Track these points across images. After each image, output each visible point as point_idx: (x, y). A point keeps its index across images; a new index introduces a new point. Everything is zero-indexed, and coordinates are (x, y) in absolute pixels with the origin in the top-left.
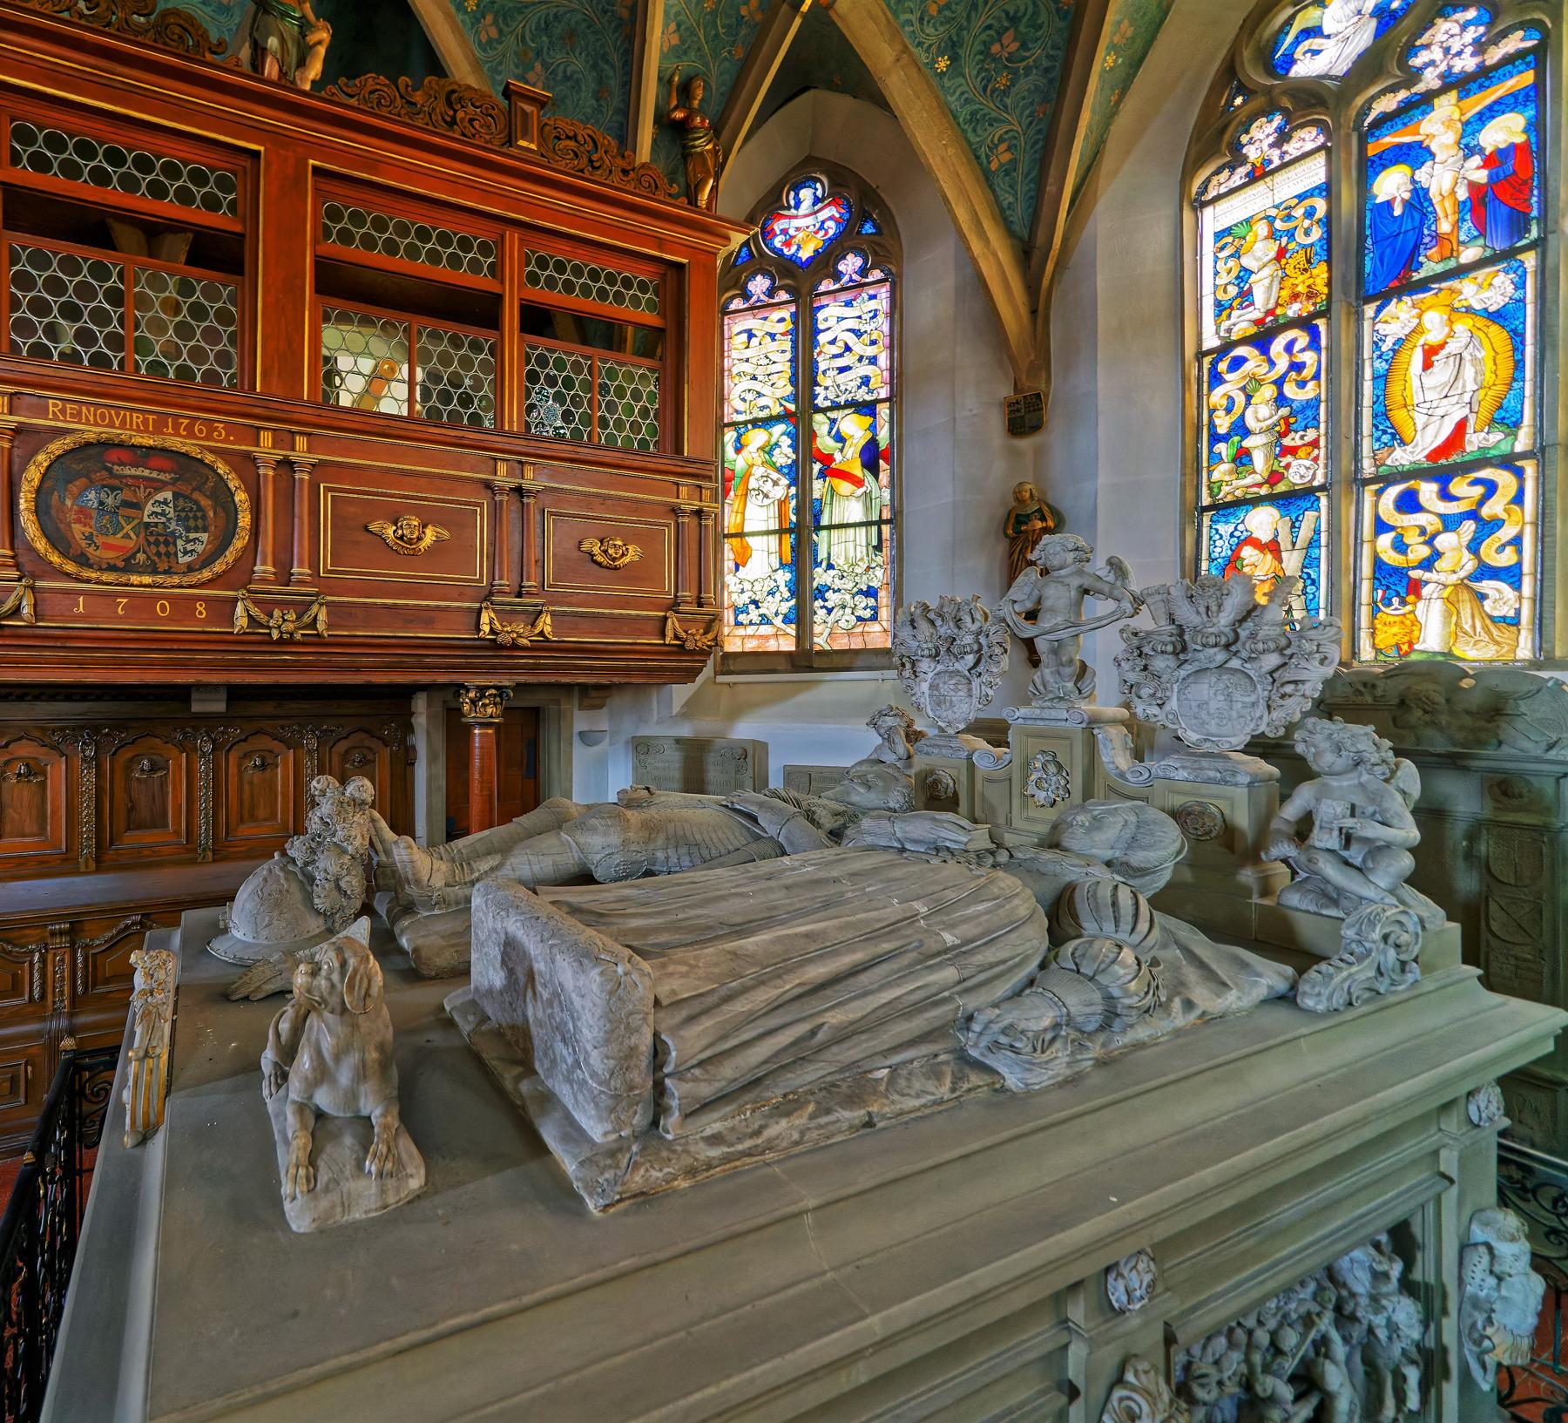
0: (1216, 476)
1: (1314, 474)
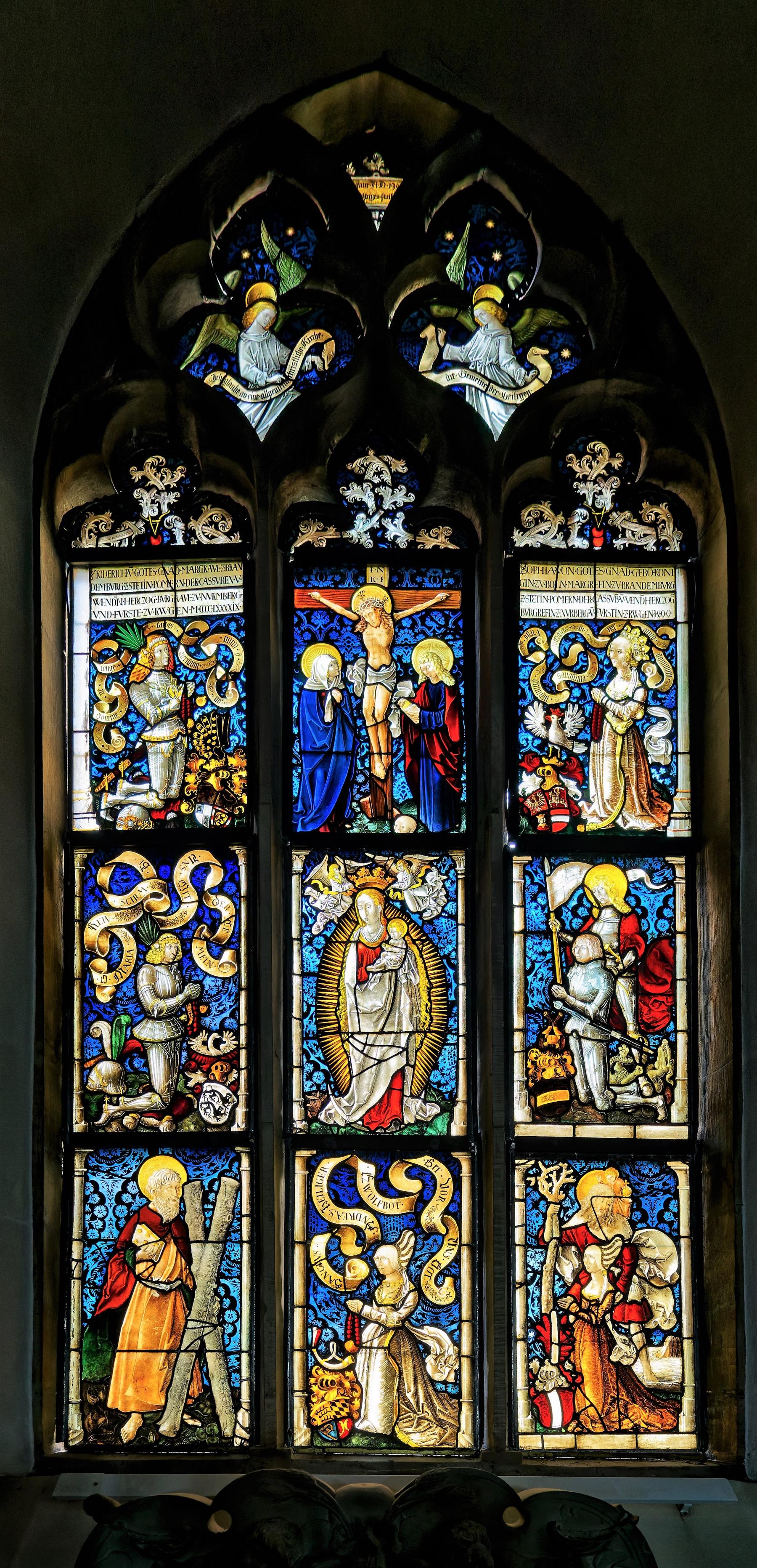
0: (95, 1080)
1: (233, 1113)
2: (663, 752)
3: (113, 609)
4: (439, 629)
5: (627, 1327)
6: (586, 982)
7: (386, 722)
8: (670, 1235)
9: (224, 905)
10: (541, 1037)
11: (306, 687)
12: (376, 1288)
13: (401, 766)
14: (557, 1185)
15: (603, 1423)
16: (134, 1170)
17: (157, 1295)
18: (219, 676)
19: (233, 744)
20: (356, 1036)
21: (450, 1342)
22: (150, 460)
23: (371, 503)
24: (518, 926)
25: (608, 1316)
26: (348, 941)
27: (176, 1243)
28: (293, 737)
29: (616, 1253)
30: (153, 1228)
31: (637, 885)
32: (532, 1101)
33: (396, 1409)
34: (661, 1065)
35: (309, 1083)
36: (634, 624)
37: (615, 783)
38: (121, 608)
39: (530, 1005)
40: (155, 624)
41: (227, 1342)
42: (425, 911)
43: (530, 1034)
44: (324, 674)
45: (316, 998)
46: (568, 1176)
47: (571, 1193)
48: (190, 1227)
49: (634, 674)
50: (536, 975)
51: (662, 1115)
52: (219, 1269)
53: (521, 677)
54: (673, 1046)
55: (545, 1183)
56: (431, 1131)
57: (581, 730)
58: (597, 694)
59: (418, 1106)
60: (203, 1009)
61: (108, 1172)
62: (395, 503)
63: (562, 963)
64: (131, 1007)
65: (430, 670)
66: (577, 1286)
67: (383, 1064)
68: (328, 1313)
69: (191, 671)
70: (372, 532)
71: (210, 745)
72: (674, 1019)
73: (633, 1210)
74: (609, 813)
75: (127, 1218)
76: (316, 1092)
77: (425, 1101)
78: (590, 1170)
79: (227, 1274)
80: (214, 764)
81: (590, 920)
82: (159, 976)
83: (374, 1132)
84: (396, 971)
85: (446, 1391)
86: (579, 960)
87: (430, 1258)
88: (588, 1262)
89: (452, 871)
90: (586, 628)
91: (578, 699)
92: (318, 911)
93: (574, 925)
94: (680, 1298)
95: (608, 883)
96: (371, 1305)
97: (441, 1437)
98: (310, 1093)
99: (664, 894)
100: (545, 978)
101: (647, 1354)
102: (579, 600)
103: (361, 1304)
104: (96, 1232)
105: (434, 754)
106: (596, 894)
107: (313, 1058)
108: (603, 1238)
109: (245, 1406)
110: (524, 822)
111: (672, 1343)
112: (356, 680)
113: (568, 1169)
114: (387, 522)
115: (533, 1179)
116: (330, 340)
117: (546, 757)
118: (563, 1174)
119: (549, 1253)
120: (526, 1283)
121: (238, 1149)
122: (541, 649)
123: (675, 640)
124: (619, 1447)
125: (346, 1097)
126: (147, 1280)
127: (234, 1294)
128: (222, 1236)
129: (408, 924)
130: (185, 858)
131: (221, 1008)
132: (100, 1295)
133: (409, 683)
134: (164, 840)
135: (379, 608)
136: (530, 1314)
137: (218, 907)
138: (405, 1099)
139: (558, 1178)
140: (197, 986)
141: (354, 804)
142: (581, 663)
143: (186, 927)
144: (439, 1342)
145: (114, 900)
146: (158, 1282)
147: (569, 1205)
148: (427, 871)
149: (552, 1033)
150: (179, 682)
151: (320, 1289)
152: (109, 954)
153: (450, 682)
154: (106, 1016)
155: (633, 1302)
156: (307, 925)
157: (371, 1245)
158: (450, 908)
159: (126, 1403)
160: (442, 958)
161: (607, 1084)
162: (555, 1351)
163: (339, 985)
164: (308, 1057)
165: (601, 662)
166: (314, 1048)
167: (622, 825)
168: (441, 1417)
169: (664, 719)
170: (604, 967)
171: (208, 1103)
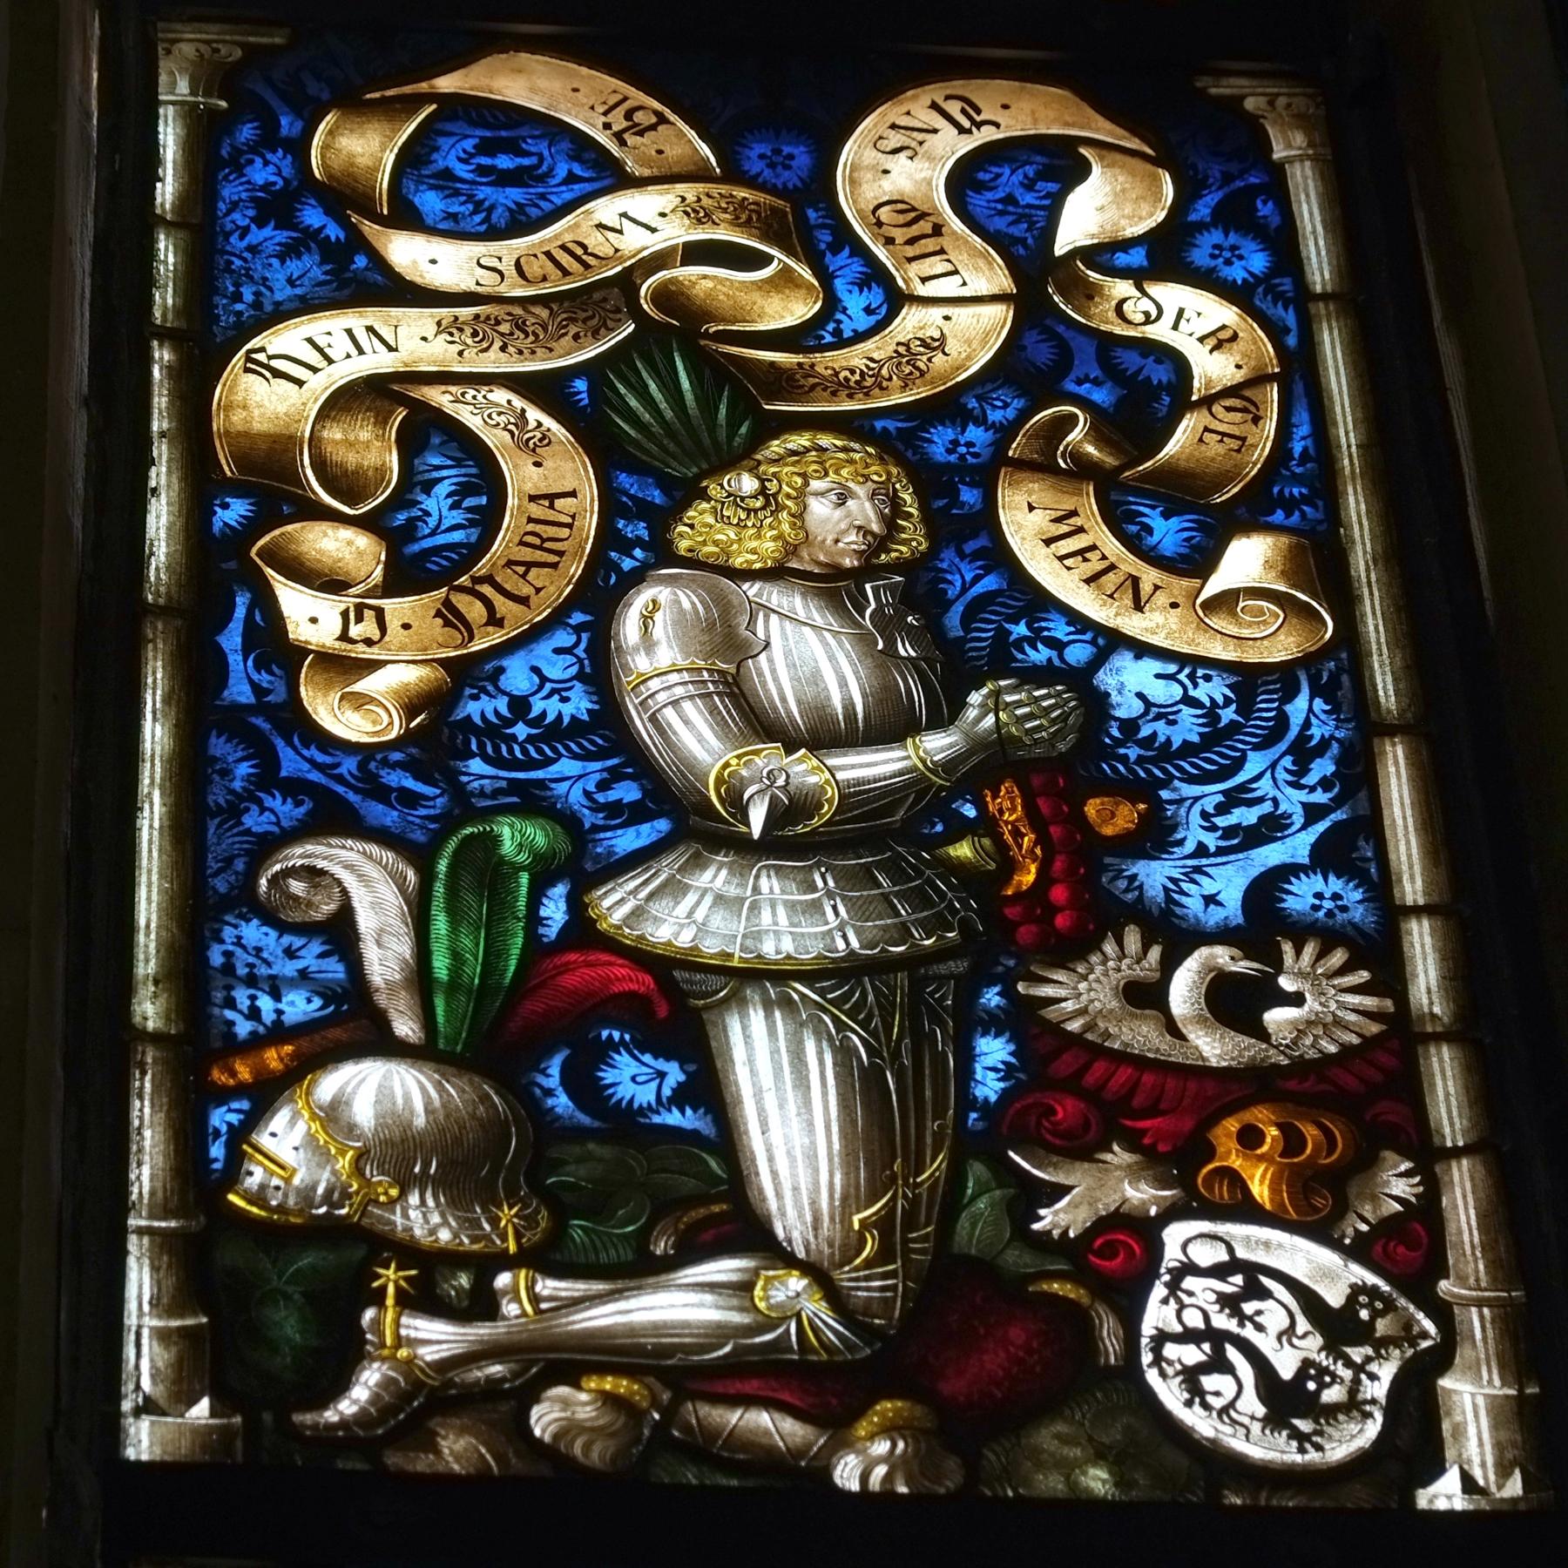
60: (1113, 817)
154: (379, 813)
171: (1217, 1338)
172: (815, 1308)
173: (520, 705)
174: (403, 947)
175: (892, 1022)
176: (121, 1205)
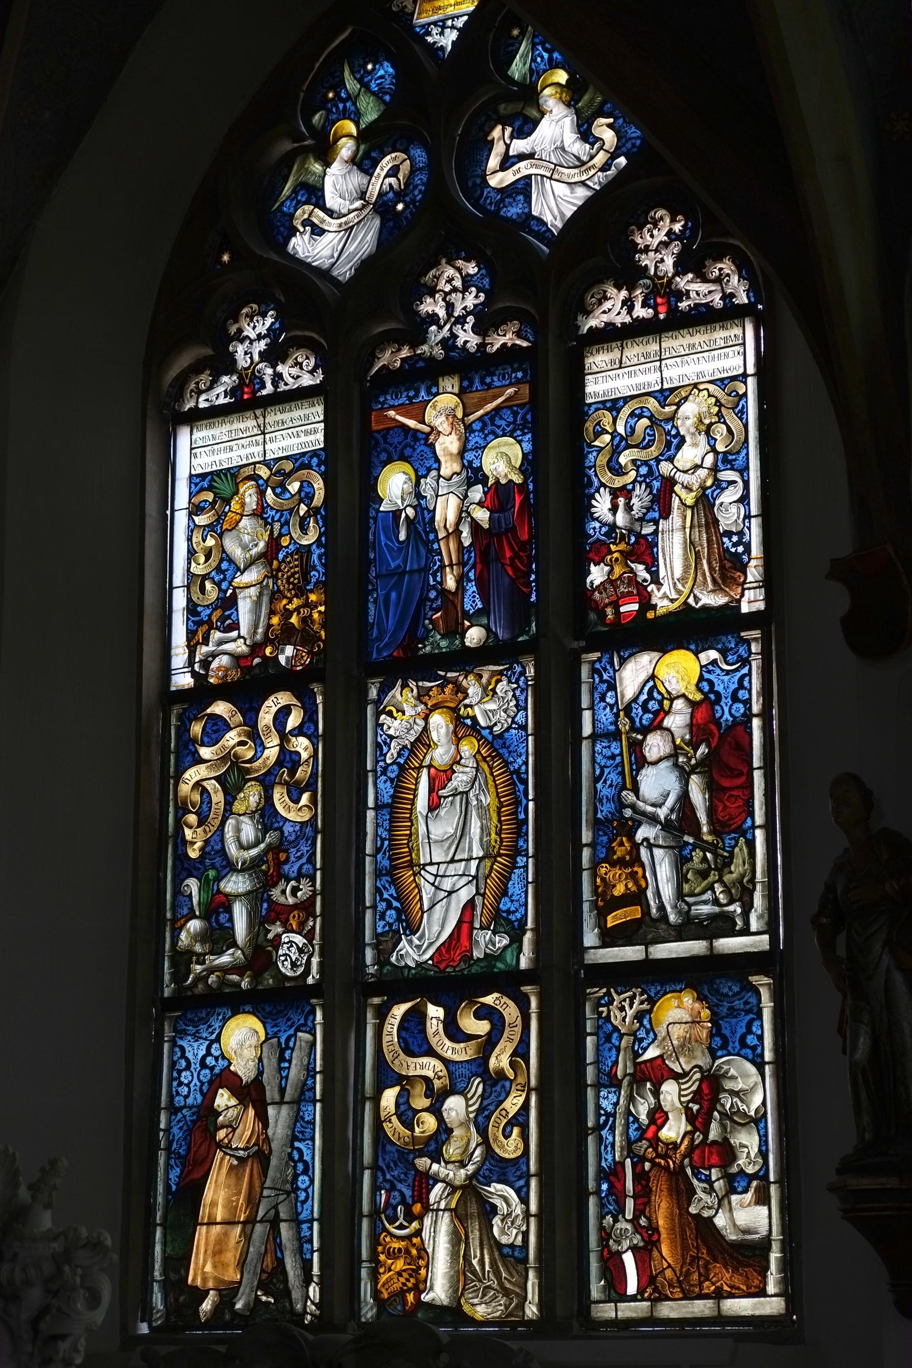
1: (308, 963)
2: (735, 517)
3: (209, 460)
4: (508, 426)
5: (707, 1173)
6: (657, 784)
7: (457, 532)
8: (753, 1062)
9: (303, 746)
10: (611, 851)
11: (382, 509)
12: (443, 1143)
13: (472, 575)
14: (630, 1013)
15: (681, 1287)
16: (217, 1032)
17: (235, 1162)
18: (302, 513)
19: (314, 580)
20: (427, 868)
21: (517, 1200)
22: (245, 311)
23: (442, 313)
24: (587, 730)
25: (687, 1161)
26: (421, 767)
27: (253, 1107)
28: (370, 562)
29: (694, 1088)
30: (234, 1093)
31: (710, 667)
32: (602, 923)
33: (462, 1278)
34: (738, 868)
35: (382, 923)
36: (701, 387)
37: (686, 559)
38: (216, 458)
39: (599, 815)
40: (246, 469)
41: (299, 1210)
42: (495, 724)
43: (599, 847)
44: (399, 493)
45: (389, 831)
46: (642, 1003)
47: (646, 1022)
48: (268, 1088)
49: (702, 438)
50: (605, 782)
51: (739, 923)
52: (294, 1131)
53: (587, 464)
54: (751, 845)
55: (617, 1013)
56: (500, 965)
57: (649, 509)
58: (665, 468)
59: (488, 938)
61: (194, 1035)
62: (465, 308)
63: (631, 764)
64: (218, 861)
65: (499, 470)
66: (653, 1128)
67: (454, 895)
68: (396, 1173)
69: (277, 511)
70: (444, 342)
71: (293, 583)
72: (752, 814)
73: (711, 1036)
74: (679, 592)
75: (210, 1082)
76: (388, 932)
77: (495, 933)
78: (665, 993)
79: (300, 1136)
80: (296, 602)
81: (663, 712)
82: (243, 826)
83: (443, 971)
84: (467, 793)
85: (513, 1256)
86: (649, 760)
87: (497, 1107)
88: (665, 1099)
89: (522, 678)
90: (652, 400)
91: (645, 476)
92: (391, 737)
93: (644, 722)
94: (766, 1135)
95: (679, 670)
96: (440, 1163)
97: (507, 1307)
98: (382, 934)
99: (739, 675)
100: (615, 783)
101: (730, 1203)
102: (645, 372)
103: (429, 1161)
104: (182, 1099)
105: (505, 558)
106: (667, 685)
107: (386, 896)
108: (680, 1071)
109: (315, 1279)
110: (593, 616)
111: (757, 1189)
112: (429, 493)
113: (642, 994)
114: (458, 330)
115: (605, 1009)
116: (405, 160)
117: (614, 543)
118: (636, 1002)
119: (623, 1093)
120: (599, 1127)
121: (314, 1001)
122: (607, 432)
123: (745, 394)
124: (699, 1315)
125: (417, 935)
126: (227, 1147)
127: (307, 1158)
128: (296, 1096)
129: (478, 741)
130: (269, 703)
131: (299, 854)
132: (184, 1166)
133: (480, 486)
134: (250, 684)
135: (451, 414)
136: (603, 1164)
137: (298, 749)
138: (475, 932)
139: (631, 1007)
140: (277, 833)
141: (427, 622)
142: (648, 438)
143: (268, 773)
144: (506, 1199)
145: (205, 752)
146: (237, 1149)
147: (644, 1035)
148: (498, 682)
149: (621, 844)
150: (266, 523)
151: (389, 1147)
152: (200, 807)
153: (517, 479)
154: (195, 873)
155: (714, 1142)
156: (381, 755)
157: (439, 1096)
158: (520, 718)
159: (205, 1280)
160: (512, 773)
161: (680, 895)
162: (630, 1204)
163: (411, 814)
164: (381, 895)
165: (668, 433)
166: (387, 885)
167: (694, 605)
168: (508, 1285)
169: (735, 482)
170: (676, 765)
171: (286, 955)
172: (241, 956)
173: (213, 847)
174: (197, 898)
175: (255, 898)
176: (164, 952)
